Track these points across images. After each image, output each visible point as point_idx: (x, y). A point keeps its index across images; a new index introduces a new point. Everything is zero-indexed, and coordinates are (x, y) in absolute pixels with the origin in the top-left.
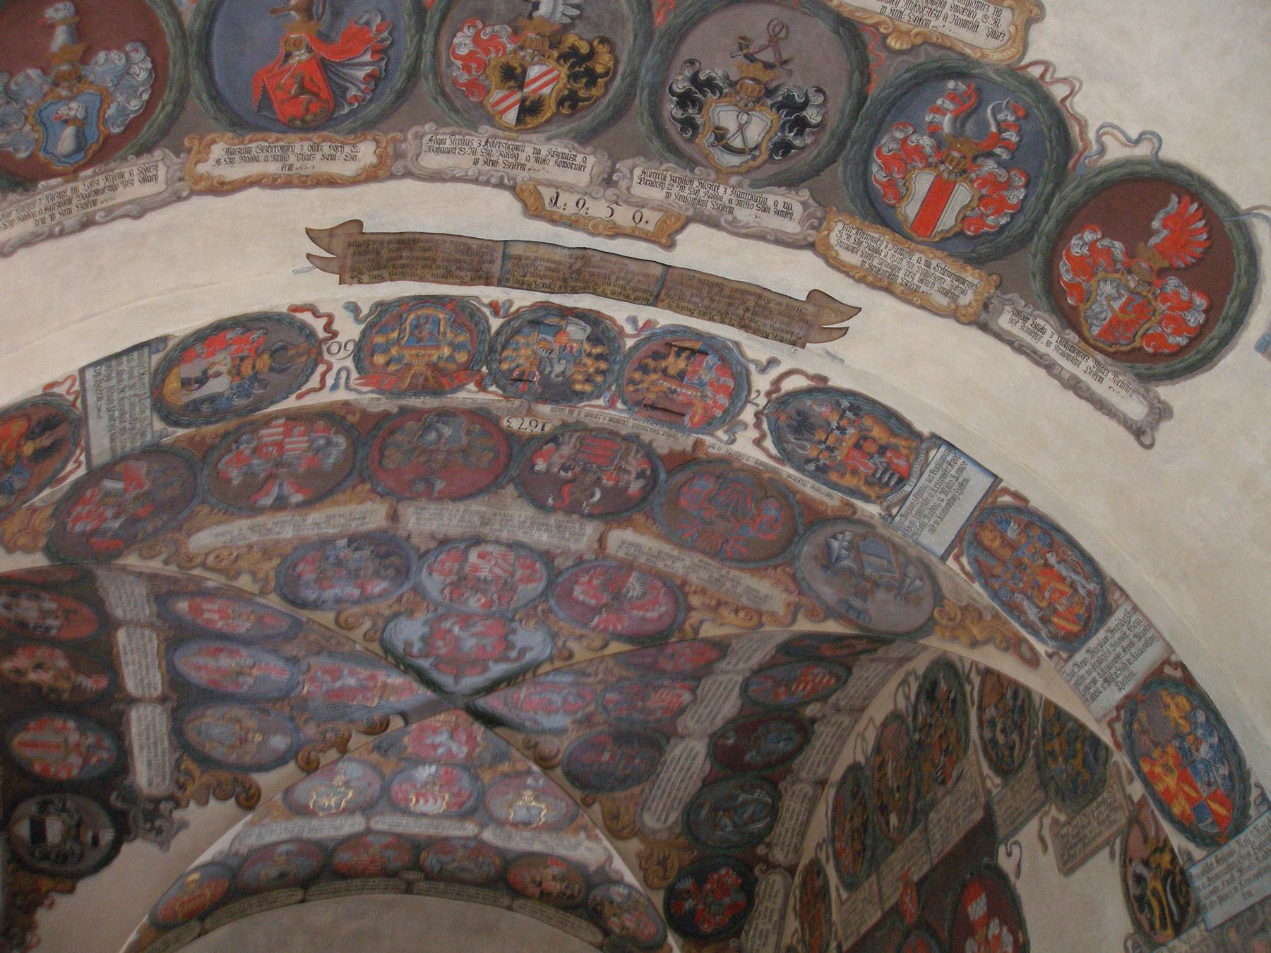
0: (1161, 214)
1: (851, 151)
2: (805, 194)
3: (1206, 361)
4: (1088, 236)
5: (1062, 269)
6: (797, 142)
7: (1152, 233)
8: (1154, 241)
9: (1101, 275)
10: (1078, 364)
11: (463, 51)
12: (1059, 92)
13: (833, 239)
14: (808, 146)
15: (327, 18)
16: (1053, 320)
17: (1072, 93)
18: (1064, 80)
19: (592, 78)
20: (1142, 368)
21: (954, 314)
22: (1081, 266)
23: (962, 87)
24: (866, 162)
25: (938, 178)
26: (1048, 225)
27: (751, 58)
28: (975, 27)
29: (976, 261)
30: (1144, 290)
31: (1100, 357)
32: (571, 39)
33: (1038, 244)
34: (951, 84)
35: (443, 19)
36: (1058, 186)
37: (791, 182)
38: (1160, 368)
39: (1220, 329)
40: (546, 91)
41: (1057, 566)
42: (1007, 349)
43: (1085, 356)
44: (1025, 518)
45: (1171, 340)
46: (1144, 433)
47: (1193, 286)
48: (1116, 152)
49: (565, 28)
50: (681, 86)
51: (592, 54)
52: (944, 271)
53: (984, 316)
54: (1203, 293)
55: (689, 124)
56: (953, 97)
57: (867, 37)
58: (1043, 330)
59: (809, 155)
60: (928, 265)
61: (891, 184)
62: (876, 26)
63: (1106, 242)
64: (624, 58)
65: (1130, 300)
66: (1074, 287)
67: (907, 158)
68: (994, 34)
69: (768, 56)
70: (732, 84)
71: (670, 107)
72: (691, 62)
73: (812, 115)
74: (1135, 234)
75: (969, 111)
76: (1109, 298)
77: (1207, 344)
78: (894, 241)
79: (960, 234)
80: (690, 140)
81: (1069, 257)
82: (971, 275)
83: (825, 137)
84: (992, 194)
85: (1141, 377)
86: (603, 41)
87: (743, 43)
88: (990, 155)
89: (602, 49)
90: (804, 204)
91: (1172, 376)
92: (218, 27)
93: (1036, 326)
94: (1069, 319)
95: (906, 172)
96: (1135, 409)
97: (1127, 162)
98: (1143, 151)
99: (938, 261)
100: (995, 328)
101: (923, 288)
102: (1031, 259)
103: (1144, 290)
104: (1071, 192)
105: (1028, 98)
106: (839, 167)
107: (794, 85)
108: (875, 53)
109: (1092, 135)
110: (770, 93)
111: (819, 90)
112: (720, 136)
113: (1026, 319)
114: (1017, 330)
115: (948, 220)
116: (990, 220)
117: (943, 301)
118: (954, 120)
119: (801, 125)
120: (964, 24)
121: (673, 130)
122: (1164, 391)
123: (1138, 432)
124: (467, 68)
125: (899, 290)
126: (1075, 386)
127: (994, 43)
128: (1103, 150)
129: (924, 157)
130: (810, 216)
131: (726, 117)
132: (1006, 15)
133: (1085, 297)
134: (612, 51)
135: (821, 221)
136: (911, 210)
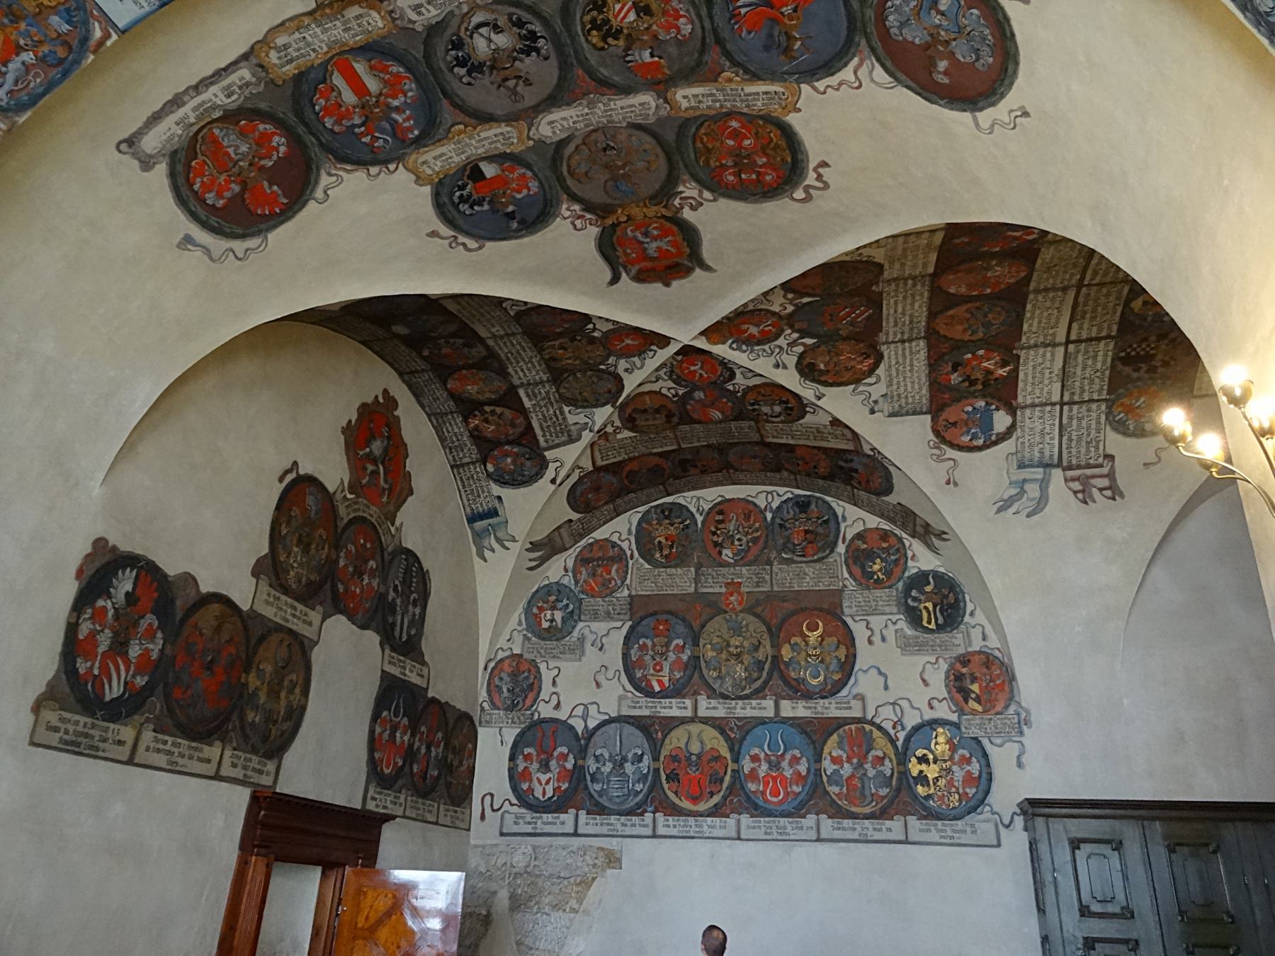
0: (280, 192)
1: (423, 68)
2: (420, 29)
3: (181, 201)
4: (282, 149)
5: (268, 126)
6: (453, 53)
7: (271, 185)
8: (266, 184)
9: (254, 147)
10: (194, 109)
11: (682, 20)
12: (374, 170)
13: (374, 14)
14: (444, 55)
15: (776, 33)
16: (234, 106)
17: (369, 174)
18: (379, 174)
19: (595, 25)
20: (181, 156)
21: (265, 42)
22: (267, 137)
23: (411, 136)
24: (409, 70)
25: (370, 94)
26: (301, 130)
27: (519, 77)
28: (435, 158)
29: (299, 78)
30: (236, 170)
31: (196, 128)
32: (621, 43)
33: (292, 119)
34: (416, 132)
35: (704, 38)
36: (321, 144)
37: (435, 29)
38: (179, 168)
39: (202, 213)
40: (618, 7)
41: (19, 59)
42: (223, 65)
43: (199, 118)
44: (75, 43)
45: (198, 180)
46: (130, 146)
47: (229, 199)
48: (325, 180)
49: (628, 48)
50: (541, 42)
51: (604, 39)
52: (303, 56)
53: (254, 61)
54: (225, 207)
55: (520, 24)
56: (410, 129)
57: (473, 121)
58: (228, 96)
59: (440, 52)
60: (314, 50)
61: (385, 69)
62: (475, 128)
63: (275, 157)
64: (585, 45)
65: (231, 159)
66: (254, 129)
67: (393, 86)
68: (424, 163)
69: (511, 83)
70: (515, 59)
71: (537, 27)
72: (546, 58)
73: (463, 71)
74: (273, 175)
75: (395, 130)
76: (237, 147)
77: (193, 204)
78: (345, 44)
79: (324, 81)
80: (510, 15)
81: (274, 134)
82: (290, 70)
83: (442, 65)
84: (337, 108)
85: (173, 155)
86: (603, 49)
87: (528, 83)
88: (363, 124)
89: (601, 44)
90: (415, 22)
91: (172, 175)
92: (844, 33)
93: (233, 93)
94: (230, 117)
95: (386, 82)
96: (152, 142)
97: (317, 182)
98: (319, 193)
99: (314, 59)
100: (243, 64)
101: (297, 35)
102: (284, 110)
103: (236, 170)
104: (315, 151)
105: (381, 156)
106: (420, 56)
107: (485, 80)
108: (462, 117)
109: (341, 173)
110: (492, 68)
111: (469, 84)
112: (497, 28)
113: (240, 88)
114: (234, 78)
115: (338, 80)
116: (322, 102)
117: (281, 40)
118: (396, 122)
119: (461, 63)
120: (442, 155)
121: (526, 16)
122: (162, 168)
123: (131, 141)
124: (677, 11)
125: (306, 20)
126: (176, 102)
127: (420, 160)
128: (330, 174)
129: (387, 96)
130: (402, 17)
131: (501, 40)
132: (429, 172)
133: (243, 134)
134: (594, 46)
135: (394, 20)
136: (360, 67)
